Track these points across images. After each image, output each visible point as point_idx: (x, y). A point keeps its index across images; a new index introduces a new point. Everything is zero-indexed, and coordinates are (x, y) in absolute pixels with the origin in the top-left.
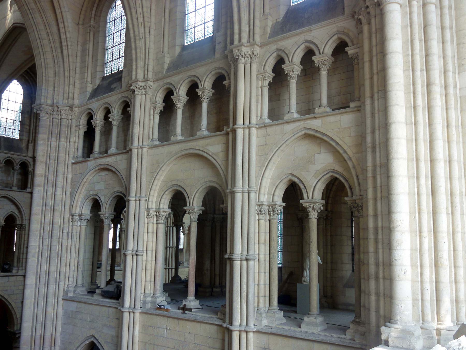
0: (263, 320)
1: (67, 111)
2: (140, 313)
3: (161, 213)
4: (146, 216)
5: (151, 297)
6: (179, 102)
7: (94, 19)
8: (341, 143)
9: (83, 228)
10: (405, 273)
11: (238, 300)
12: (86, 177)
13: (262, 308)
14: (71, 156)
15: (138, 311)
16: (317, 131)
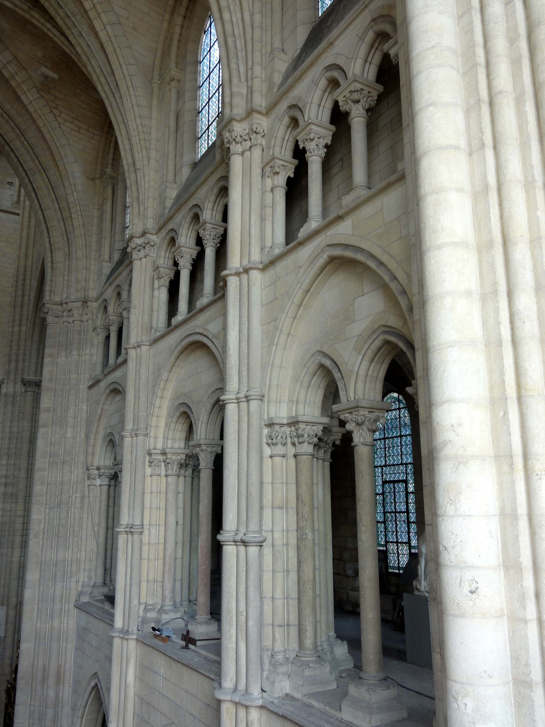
0: (277, 681)
1: (81, 309)
2: (137, 640)
3: (169, 456)
4: (147, 463)
5: (157, 610)
6: (182, 257)
7: (113, 165)
8: (384, 258)
9: (105, 488)
10: (472, 592)
11: (230, 630)
12: (100, 406)
13: (279, 652)
14: (87, 376)
15: (131, 637)
16: (347, 246)
